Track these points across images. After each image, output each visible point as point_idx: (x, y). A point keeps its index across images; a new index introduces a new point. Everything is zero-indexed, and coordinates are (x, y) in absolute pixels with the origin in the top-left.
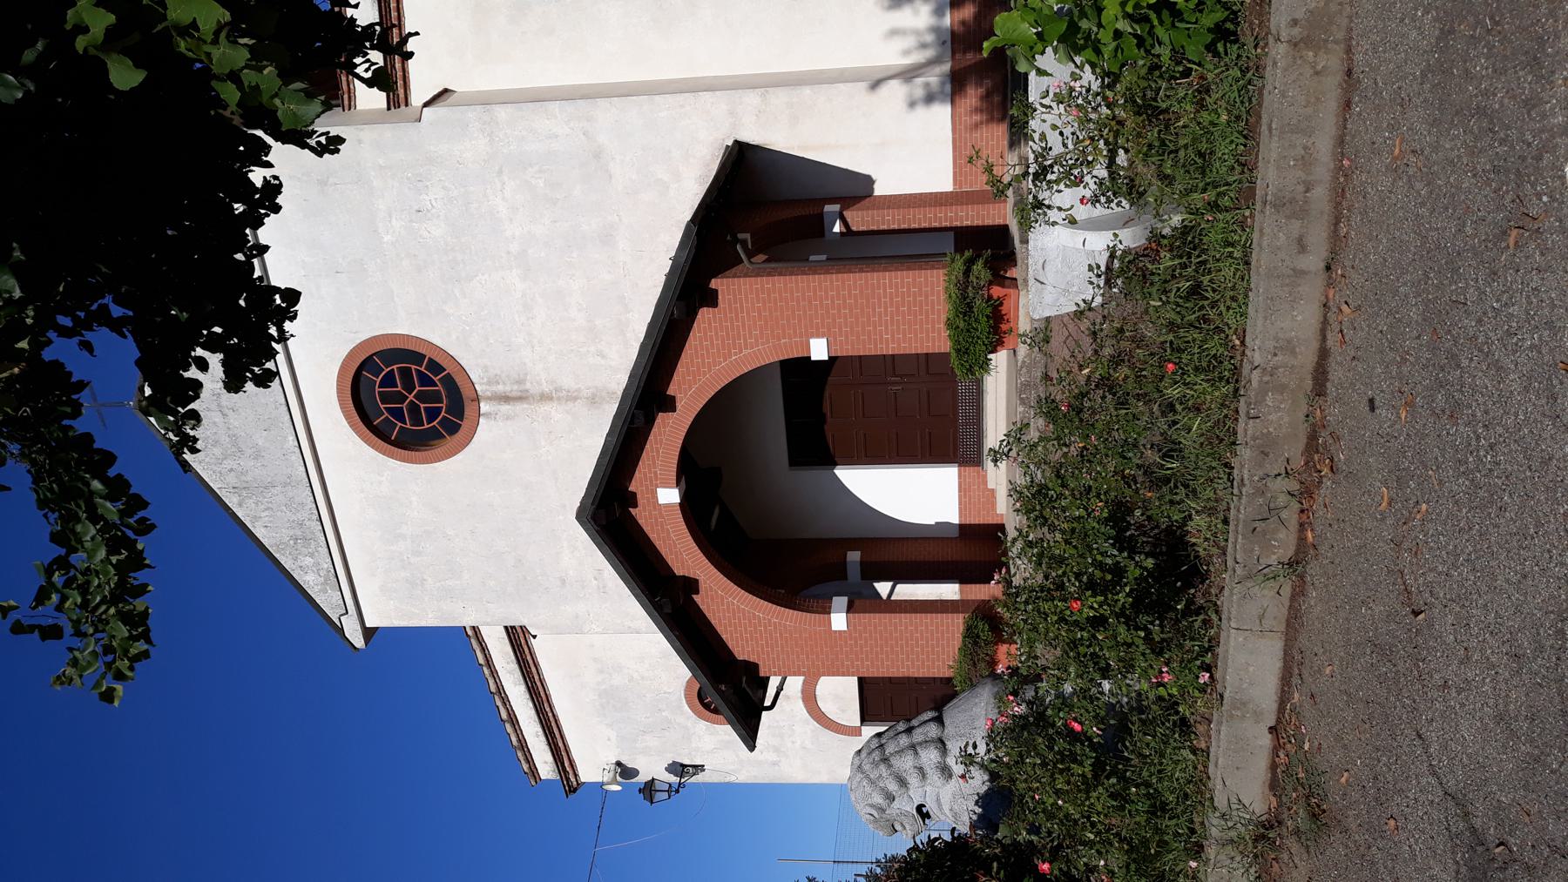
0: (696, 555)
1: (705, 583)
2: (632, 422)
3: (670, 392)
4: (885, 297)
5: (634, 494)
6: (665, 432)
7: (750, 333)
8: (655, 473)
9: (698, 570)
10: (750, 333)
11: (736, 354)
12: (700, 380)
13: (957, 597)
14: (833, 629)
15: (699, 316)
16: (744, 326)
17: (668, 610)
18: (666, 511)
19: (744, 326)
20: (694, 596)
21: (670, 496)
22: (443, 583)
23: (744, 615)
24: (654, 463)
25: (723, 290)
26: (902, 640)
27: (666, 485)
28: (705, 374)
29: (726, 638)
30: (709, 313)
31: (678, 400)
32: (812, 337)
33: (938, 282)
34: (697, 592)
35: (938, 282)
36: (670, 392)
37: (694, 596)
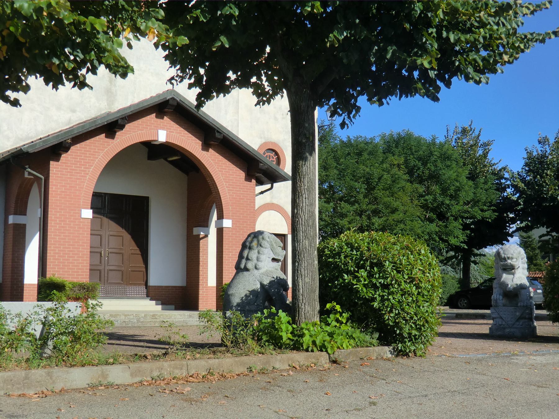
0: (124, 144)
1: (112, 143)
2: (218, 132)
3: (210, 150)
4: (70, 248)
5: (163, 118)
6: (193, 142)
7: (235, 193)
8: (173, 132)
9: (120, 141)
10: (235, 193)
11: (226, 185)
12: (215, 165)
13: (209, 285)
14: (231, 221)
15: (242, 172)
16: (237, 191)
17: (217, 135)
18: (153, 132)
19: (237, 191)
20: (104, 135)
21: (162, 137)
22: (432, 74)
23: (92, 160)
24: (178, 133)
25: (251, 184)
26: (79, 248)
27: (167, 136)
28: (218, 168)
29: (77, 147)
30: (243, 176)
31: (207, 153)
32: (232, 221)
33: (83, 278)
34: (106, 137)
35: (83, 278)
36: (210, 150)
37: (104, 135)
